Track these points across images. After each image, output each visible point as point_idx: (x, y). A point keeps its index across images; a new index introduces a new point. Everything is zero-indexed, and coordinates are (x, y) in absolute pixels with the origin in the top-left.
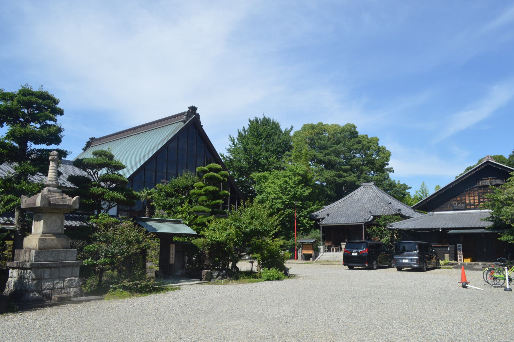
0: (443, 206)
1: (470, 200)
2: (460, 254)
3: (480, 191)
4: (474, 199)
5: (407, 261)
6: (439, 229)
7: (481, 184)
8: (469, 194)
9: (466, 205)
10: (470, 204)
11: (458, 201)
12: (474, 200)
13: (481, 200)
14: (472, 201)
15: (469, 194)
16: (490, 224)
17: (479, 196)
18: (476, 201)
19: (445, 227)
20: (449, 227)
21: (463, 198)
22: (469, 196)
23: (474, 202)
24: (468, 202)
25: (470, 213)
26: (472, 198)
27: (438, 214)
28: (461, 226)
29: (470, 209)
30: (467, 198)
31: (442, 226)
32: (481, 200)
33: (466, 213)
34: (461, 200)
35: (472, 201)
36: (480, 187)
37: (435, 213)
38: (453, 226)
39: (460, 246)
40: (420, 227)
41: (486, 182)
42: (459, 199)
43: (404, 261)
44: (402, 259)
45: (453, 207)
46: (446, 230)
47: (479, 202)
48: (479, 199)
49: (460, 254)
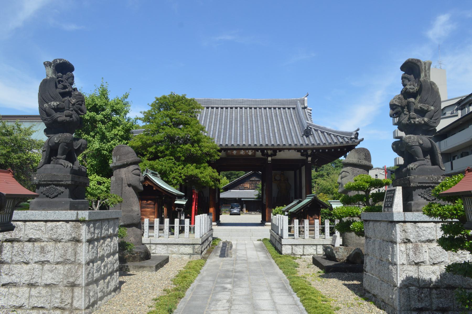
0: (236, 188)
2: (244, 209)
3: (250, 182)
4: (247, 185)
5: (236, 211)
6: (236, 198)
7: (251, 179)
9: (245, 188)
10: (246, 188)
11: (241, 186)
14: (247, 186)
16: (256, 197)
17: (250, 184)
18: (249, 186)
19: (239, 197)
20: (241, 197)
21: (244, 185)
24: (245, 186)
25: (246, 191)
26: (247, 185)
27: (233, 191)
29: (246, 190)
30: (245, 185)
31: (238, 197)
33: (244, 191)
34: (243, 186)
36: (251, 181)
37: (232, 190)
38: (242, 197)
40: (228, 197)
41: (253, 179)
42: (242, 185)
43: (234, 211)
44: (234, 211)
45: (239, 188)
46: (240, 199)
47: (250, 187)
49: (244, 209)
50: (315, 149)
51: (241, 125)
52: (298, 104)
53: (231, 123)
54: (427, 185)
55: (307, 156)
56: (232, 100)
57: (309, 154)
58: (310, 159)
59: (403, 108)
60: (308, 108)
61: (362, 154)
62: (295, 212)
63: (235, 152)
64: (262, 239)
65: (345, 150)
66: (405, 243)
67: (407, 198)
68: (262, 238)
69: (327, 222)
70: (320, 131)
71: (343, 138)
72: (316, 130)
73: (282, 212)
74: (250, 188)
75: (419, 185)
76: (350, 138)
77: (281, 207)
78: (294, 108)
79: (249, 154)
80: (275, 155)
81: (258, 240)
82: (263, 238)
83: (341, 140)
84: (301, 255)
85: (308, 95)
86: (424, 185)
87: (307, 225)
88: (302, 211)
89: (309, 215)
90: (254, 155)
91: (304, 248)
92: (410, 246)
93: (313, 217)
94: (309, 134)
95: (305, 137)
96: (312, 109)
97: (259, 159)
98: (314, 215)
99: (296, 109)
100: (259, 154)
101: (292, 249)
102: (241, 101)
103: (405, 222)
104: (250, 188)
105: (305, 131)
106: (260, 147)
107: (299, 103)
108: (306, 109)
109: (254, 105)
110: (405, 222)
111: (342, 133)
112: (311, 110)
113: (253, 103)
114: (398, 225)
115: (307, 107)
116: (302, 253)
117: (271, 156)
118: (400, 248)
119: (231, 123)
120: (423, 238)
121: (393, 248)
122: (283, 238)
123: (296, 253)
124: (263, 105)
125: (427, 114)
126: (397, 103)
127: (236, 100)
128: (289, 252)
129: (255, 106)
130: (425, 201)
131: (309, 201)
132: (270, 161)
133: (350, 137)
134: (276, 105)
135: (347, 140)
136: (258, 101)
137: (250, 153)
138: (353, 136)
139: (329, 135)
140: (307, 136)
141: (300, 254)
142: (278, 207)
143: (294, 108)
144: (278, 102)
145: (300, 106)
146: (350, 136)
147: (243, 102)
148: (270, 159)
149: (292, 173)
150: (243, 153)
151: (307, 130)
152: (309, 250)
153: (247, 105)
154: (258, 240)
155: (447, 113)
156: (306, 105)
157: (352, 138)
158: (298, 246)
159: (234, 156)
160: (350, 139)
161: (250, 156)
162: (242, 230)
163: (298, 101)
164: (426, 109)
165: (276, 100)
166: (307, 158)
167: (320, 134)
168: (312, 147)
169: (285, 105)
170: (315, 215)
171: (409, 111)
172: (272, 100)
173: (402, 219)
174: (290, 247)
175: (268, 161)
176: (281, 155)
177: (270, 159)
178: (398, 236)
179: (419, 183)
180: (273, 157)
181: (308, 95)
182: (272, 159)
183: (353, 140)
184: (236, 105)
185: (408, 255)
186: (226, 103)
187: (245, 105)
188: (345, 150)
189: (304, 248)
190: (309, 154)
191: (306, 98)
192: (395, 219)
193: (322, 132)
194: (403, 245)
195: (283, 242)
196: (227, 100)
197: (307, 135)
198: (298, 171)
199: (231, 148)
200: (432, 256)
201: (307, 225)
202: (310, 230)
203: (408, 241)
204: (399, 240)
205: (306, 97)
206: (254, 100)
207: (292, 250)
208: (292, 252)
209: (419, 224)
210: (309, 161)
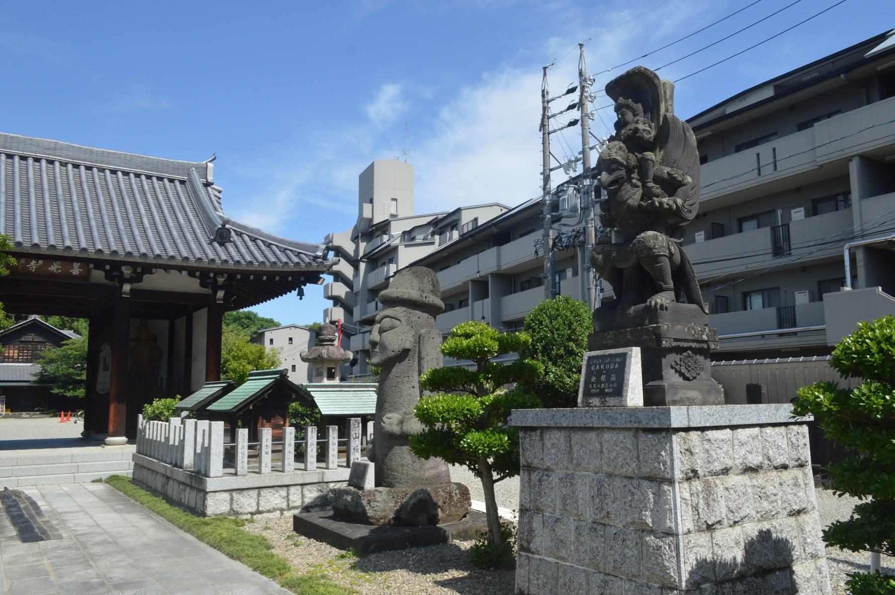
1: (9, 353)
3: (21, 346)
4: (13, 353)
7: (23, 339)
8: (9, 347)
9: (5, 357)
10: (8, 357)
12: (14, 353)
13: (21, 354)
14: (11, 355)
15: (9, 347)
16: (34, 379)
17: (19, 349)
18: (16, 355)
22: (9, 350)
23: (13, 356)
25: (7, 366)
28: (6, 379)
32: (21, 354)
33: (4, 366)
35: (11, 355)
36: (22, 342)
39: (3, 398)
41: (29, 337)
47: (19, 356)
48: (18, 353)
50: (239, 274)
51: (56, 202)
52: (193, 174)
53: (26, 193)
54: (686, 345)
55: (216, 288)
56: (25, 139)
57: (219, 284)
58: (221, 294)
59: (629, 171)
60: (214, 186)
61: (426, 280)
62: (235, 410)
63: (33, 265)
64: (104, 478)
65: (302, 279)
66: (688, 479)
67: (651, 371)
68: (104, 475)
69: (312, 432)
70: (248, 236)
71: (298, 255)
72: (240, 234)
73: (171, 411)
74: (18, 359)
75: (674, 344)
76: (313, 256)
77: (169, 400)
78: (182, 182)
79: (74, 273)
80: (139, 279)
81: (93, 481)
82: (108, 476)
83: (296, 260)
84: (252, 514)
85: (215, 159)
86: (682, 344)
87: (267, 440)
88: (251, 408)
89: (265, 417)
90: (86, 276)
91: (259, 495)
92: (697, 485)
93: (272, 421)
94: (225, 240)
95: (216, 244)
96: (221, 189)
97: (98, 286)
98: (274, 417)
99: (188, 184)
100: (98, 275)
101: (232, 499)
102: (52, 146)
103: (687, 430)
104: (18, 359)
105: (217, 231)
106: (109, 258)
107: (195, 172)
108: (209, 188)
109: (85, 160)
110: (687, 430)
111: (297, 245)
112: (220, 192)
113: (82, 156)
114: (676, 439)
115: (212, 184)
116: (254, 509)
117: (129, 281)
118: (682, 492)
119: (26, 193)
120: (717, 466)
121: (659, 495)
122: (209, 477)
123: (241, 511)
124: (108, 164)
125: (680, 191)
126: (619, 158)
127: (37, 141)
128: (225, 508)
129: (89, 164)
130: (681, 379)
131: (267, 384)
132: (127, 294)
133: (314, 255)
134: (142, 169)
135: (307, 260)
136: (97, 153)
137: (76, 270)
138: (320, 254)
139: (269, 246)
140: (222, 244)
141: (250, 510)
142: (160, 400)
143: (182, 182)
144: (147, 164)
145: (199, 182)
146: (314, 252)
147: (55, 149)
148: (127, 287)
149: (163, 326)
150: (58, 269)
151: (223, 230)
152: (272, 499)
153: (68, 158)
154: (93, 481)
155: (418, 237)
156: (210, 179)
157: (316, 257)
158: (245, 493)
159: (30, 273)
160: (312, 258)
161: (75, 276)
162: (48, 457)
163: (194, 169)
164: (680, 179)
165: (141, 157)
166: (215, 293)
167: (250, 243)
168: (235, 268)
169: (162, 172)
170: (277, 417)
171: (643, 179)
172: (131, 156)
173: (684, 424)
174: (226, 496)
175: (121, 293)
176: (157, 281)
177: (127, 287)
178: (677, 464)
179: (676, 340)
180: (137, 286)
181: (215, 159)
182: (131, 290)
183: (320, 260)
184: (36, 152)
185: (696, 508)
186: (8, 145)
187: (60, 156)
188: (302, 279)
189: (259, 495)
190: (219, 284)
191: (210, 165)
192: (675, 425)
193: (254, 240)
194: (686, 485)
195: (211, 484)
196: (12, 137)
197: (220, 241)
198: (181, 323)
199: (30, 252)
200: (733, 506)
201: (267, 440)
202: (273, 452)
203: (692, 475)
204: (678, 475)
205: (210, 161)
206: (86, 149)
207: (231, 504)
208: (232, 509)
209: (710, 434)
210: (219, 299)
